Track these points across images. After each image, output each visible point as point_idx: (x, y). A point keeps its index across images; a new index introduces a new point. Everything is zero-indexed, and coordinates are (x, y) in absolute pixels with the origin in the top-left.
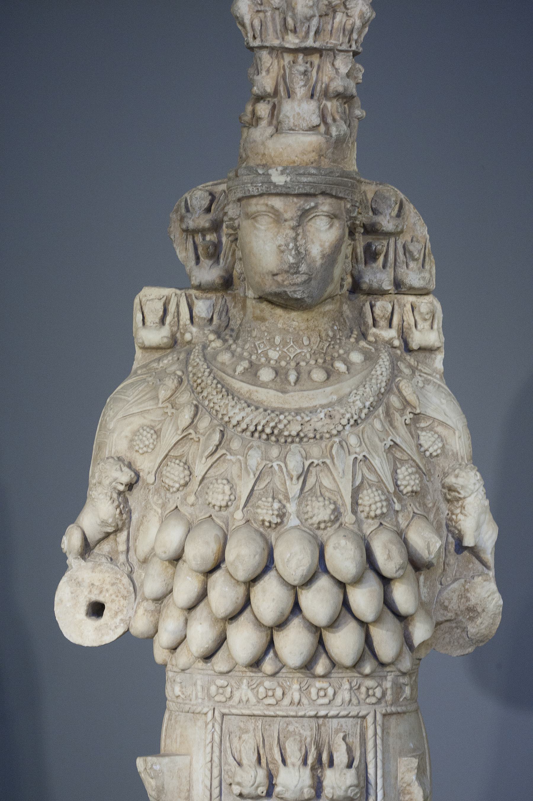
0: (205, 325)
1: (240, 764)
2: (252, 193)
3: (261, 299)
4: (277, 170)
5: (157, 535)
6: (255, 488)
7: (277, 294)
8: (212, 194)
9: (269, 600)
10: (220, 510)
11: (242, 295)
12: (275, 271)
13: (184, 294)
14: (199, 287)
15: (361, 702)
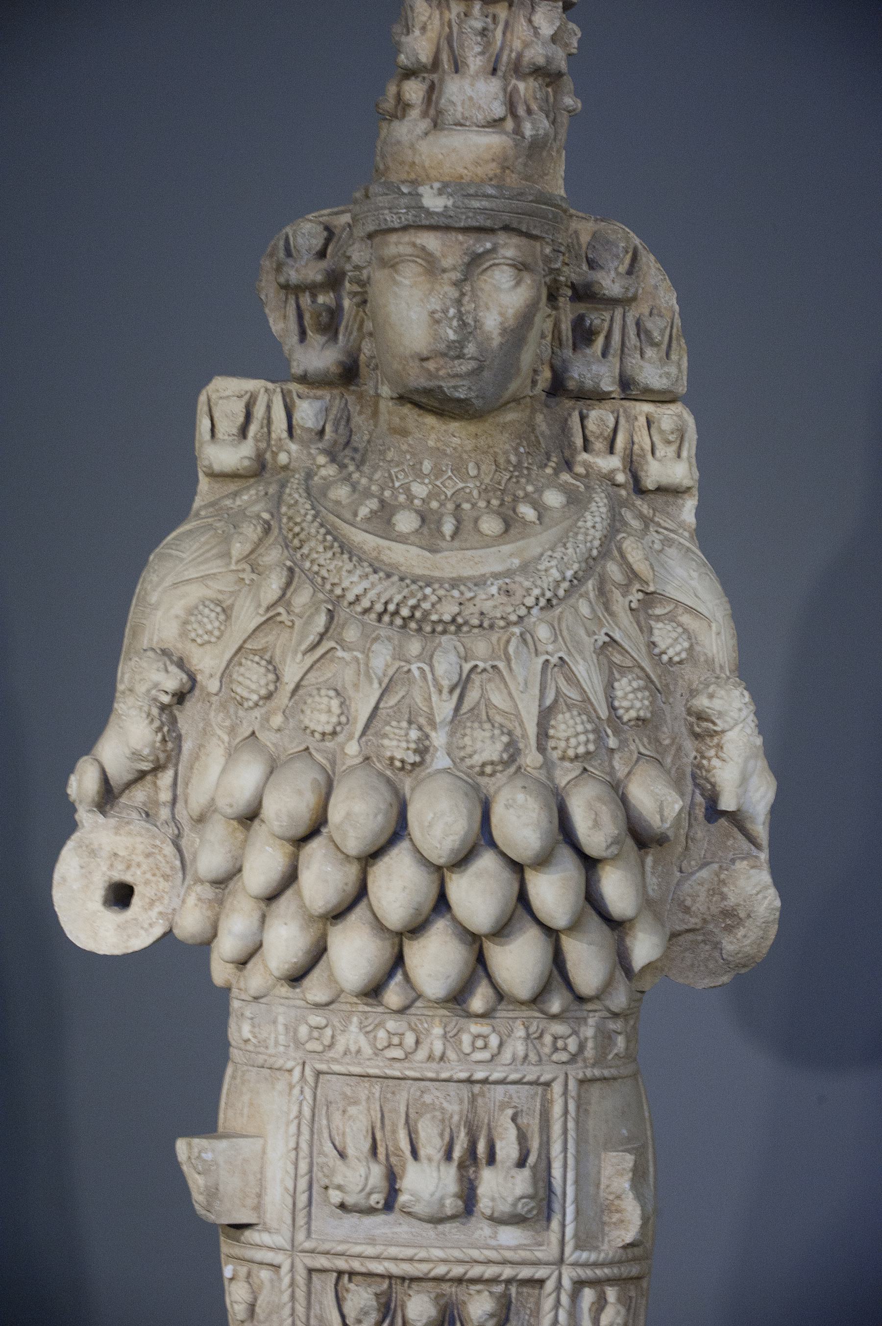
0: (311, 441)
1: (342, 1155)
2: (391, 225)
3: (402, 399)
4: (432, 187)
5: (221, 776)
6: (382, 705)
7: (428, 392)
8: (327, 228)
9: (397, 888)
10: (323, 740)
11: (372, 392)
12: (425, 353)
13: (279, 390)
14: (304, 379)
15: (544, 1058)
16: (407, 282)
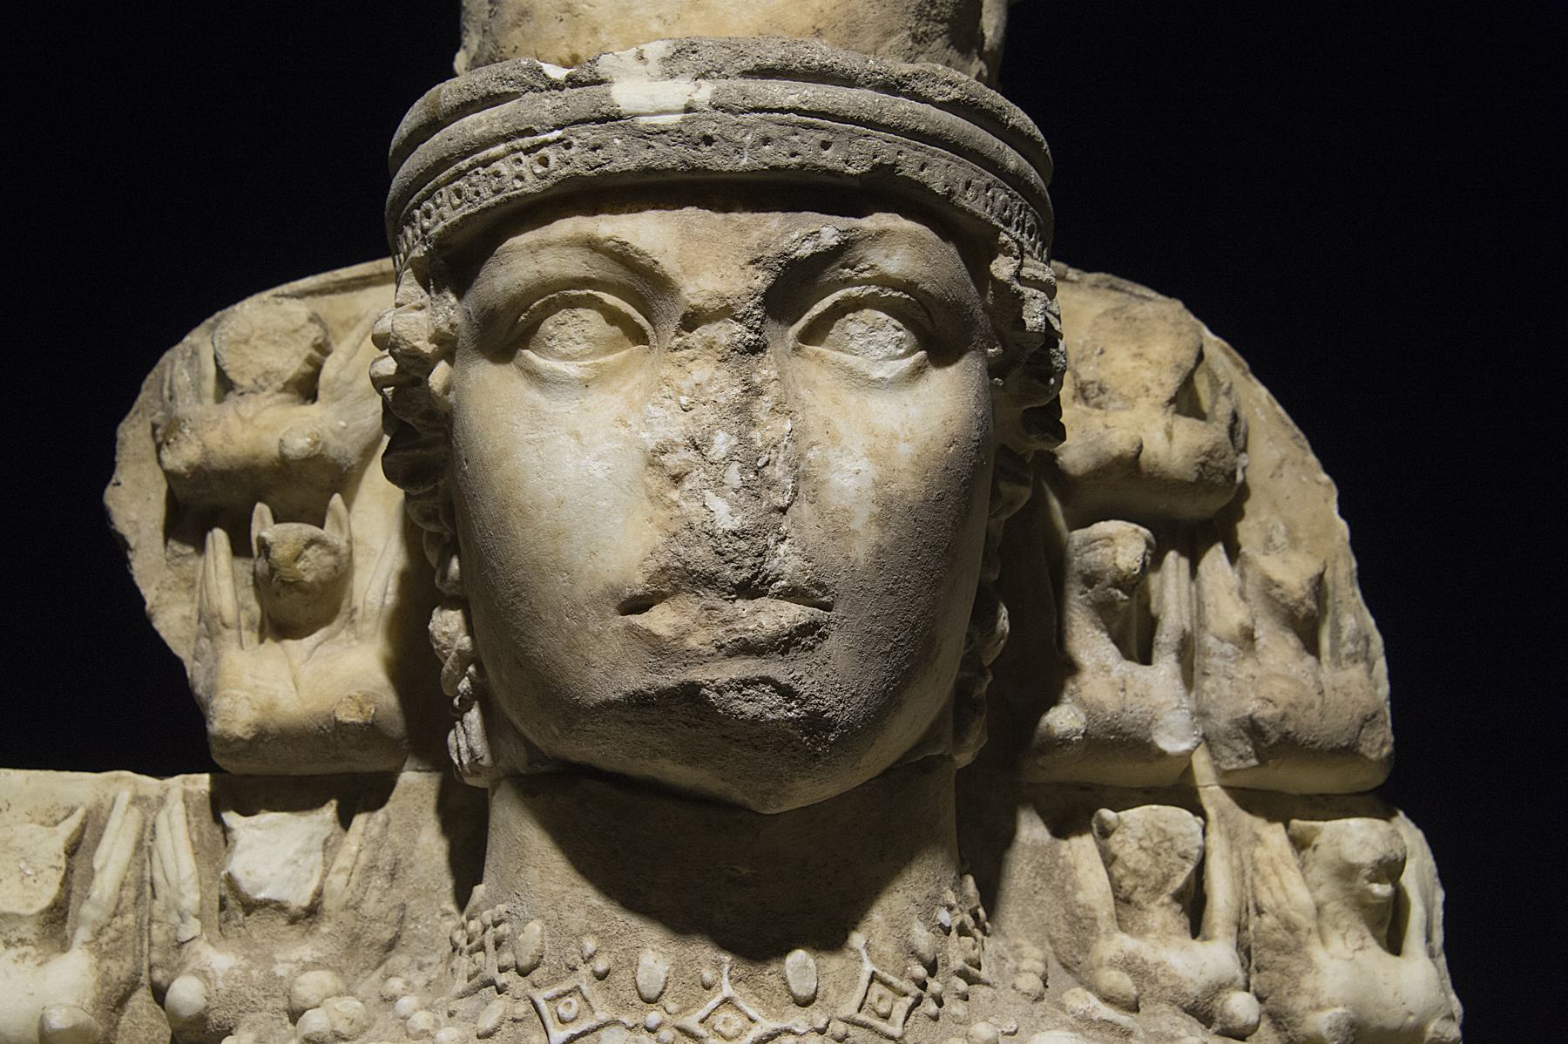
12: (638, 582)
16: (571, 369)
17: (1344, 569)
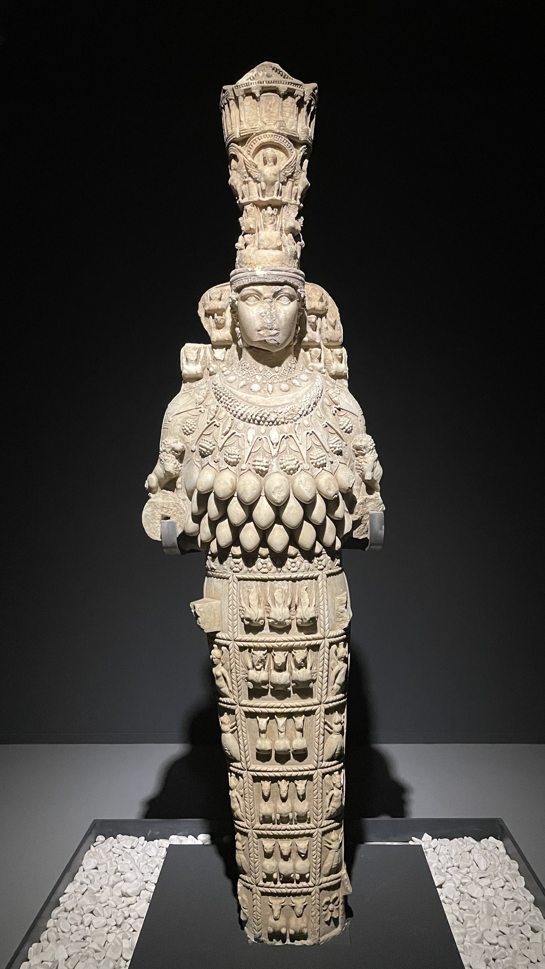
12: (259, 329)
17: (339, 318)
